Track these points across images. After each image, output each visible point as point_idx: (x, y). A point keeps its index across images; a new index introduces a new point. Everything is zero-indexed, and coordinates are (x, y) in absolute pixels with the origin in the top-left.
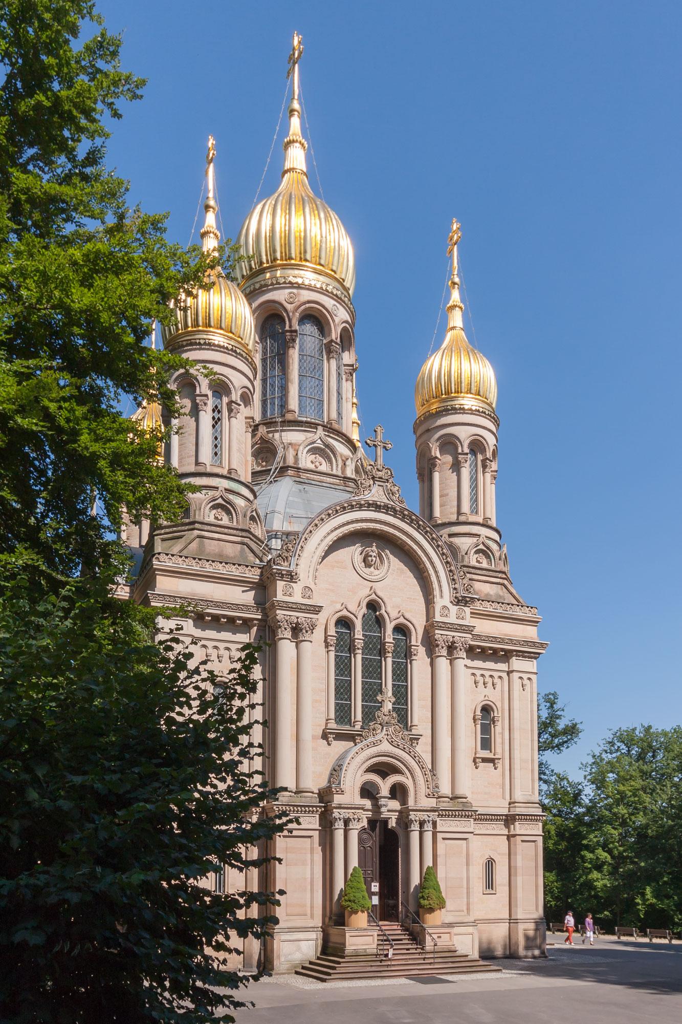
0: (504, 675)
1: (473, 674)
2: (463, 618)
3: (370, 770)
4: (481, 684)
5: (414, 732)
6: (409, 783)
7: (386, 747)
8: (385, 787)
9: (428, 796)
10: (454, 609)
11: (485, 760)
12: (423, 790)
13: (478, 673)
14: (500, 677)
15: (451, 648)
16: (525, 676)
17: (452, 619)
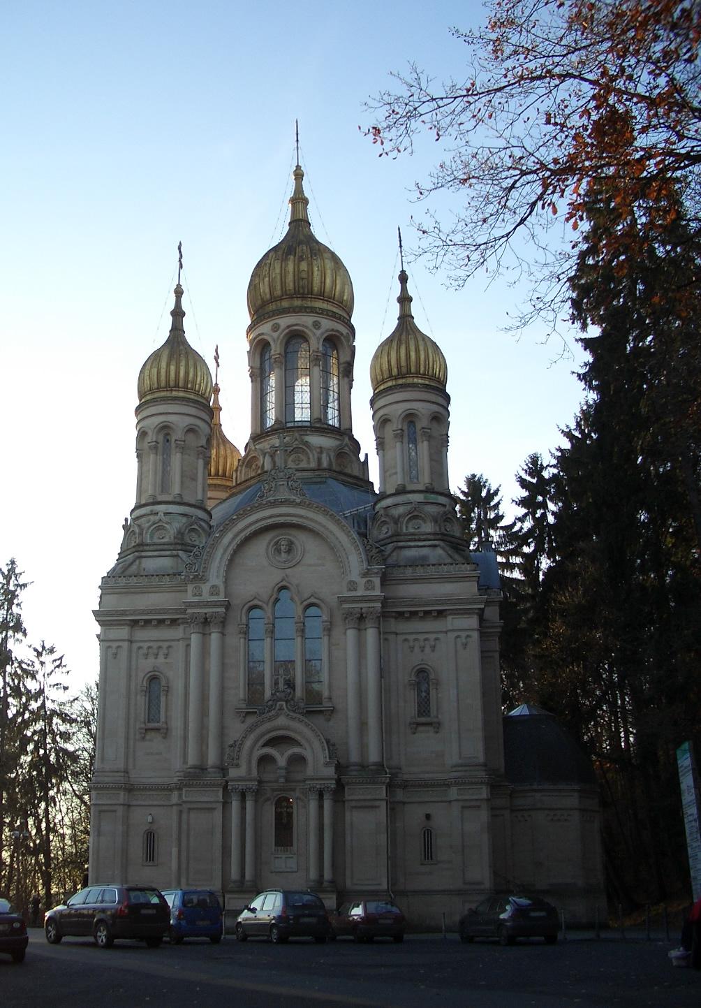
0: (439, 636)
1: (406, 640)
2: (373, 589)
3: (265, 745)
4: (417, 650)
5: (326, 704)
6: (307, 754)
7: (282, 721)
8: (282, 761)
9: (326, 764)
10: (362, 582)
11: (418, 724)
12: (322, 761)
13: (411, 637)
14: (437, 639)
15: (362, 618)
16: (463, 634)
17: (360, 592)
